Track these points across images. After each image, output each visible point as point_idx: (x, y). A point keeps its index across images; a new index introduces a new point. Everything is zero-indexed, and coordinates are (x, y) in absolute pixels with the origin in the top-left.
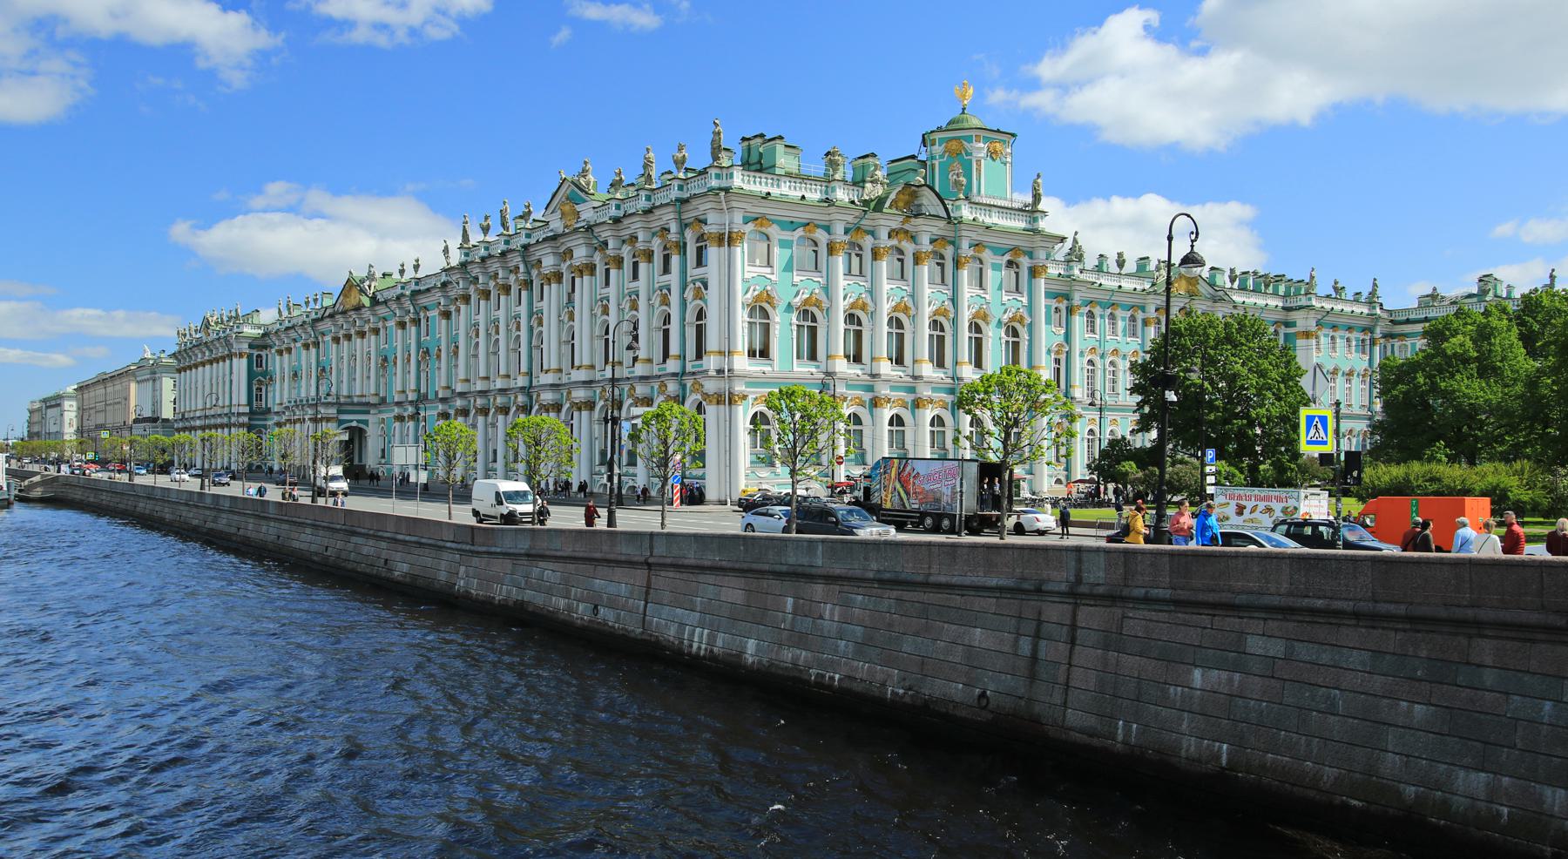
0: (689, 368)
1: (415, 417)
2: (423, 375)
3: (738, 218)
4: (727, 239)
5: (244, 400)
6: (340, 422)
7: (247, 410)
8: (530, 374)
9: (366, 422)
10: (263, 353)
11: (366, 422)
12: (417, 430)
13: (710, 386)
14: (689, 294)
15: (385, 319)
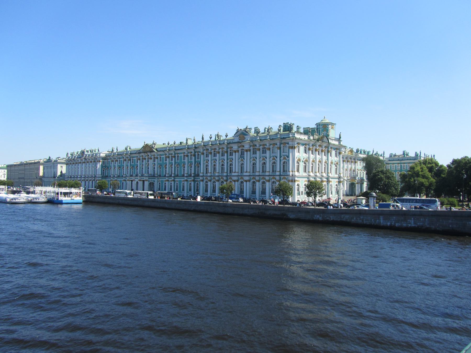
0: (281, 174)
1: (174, 181)
2: (176, 170)
3: (296, 143)
4: (293, 148)
5: (100, 174)
6: (149, 181)
7: (101, 176)
8: (227, 172)
9: (154, 181)
10: (105, 161)
11: (154, 181)
12: (174, 184)
13: (290, 179)
14: (282, 158)
15: (161, 155)
